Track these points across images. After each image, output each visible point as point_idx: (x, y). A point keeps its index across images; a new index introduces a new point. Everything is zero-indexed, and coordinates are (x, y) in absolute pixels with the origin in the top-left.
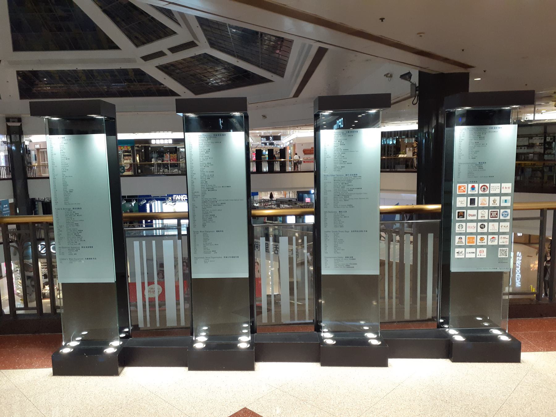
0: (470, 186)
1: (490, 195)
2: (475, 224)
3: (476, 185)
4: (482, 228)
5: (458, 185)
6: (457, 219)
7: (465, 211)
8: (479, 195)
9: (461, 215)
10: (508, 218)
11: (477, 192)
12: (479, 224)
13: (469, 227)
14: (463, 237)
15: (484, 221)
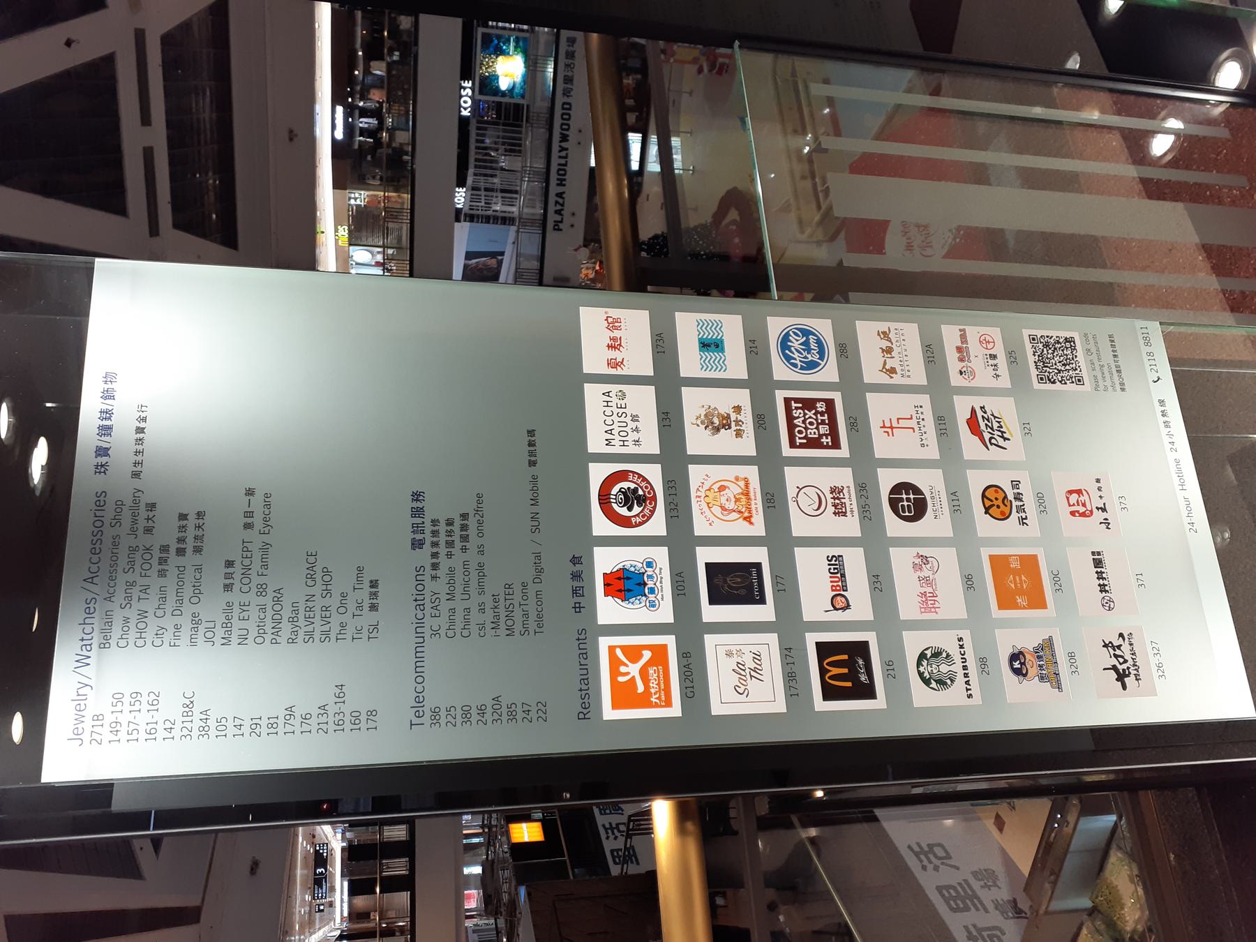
0: (609, 610)
1: (674, 456)
2: (901, 560)
3: (605, 561)
4: (919, 510)
5: (609, 713)
6: (880, 703)
7: (812, 639)
8: (681, 539)
9: (847, 669)
10: (823, 327)
11: (661, 555)
12: (894, 526)
13: (928, 600)
15: (865, 488)
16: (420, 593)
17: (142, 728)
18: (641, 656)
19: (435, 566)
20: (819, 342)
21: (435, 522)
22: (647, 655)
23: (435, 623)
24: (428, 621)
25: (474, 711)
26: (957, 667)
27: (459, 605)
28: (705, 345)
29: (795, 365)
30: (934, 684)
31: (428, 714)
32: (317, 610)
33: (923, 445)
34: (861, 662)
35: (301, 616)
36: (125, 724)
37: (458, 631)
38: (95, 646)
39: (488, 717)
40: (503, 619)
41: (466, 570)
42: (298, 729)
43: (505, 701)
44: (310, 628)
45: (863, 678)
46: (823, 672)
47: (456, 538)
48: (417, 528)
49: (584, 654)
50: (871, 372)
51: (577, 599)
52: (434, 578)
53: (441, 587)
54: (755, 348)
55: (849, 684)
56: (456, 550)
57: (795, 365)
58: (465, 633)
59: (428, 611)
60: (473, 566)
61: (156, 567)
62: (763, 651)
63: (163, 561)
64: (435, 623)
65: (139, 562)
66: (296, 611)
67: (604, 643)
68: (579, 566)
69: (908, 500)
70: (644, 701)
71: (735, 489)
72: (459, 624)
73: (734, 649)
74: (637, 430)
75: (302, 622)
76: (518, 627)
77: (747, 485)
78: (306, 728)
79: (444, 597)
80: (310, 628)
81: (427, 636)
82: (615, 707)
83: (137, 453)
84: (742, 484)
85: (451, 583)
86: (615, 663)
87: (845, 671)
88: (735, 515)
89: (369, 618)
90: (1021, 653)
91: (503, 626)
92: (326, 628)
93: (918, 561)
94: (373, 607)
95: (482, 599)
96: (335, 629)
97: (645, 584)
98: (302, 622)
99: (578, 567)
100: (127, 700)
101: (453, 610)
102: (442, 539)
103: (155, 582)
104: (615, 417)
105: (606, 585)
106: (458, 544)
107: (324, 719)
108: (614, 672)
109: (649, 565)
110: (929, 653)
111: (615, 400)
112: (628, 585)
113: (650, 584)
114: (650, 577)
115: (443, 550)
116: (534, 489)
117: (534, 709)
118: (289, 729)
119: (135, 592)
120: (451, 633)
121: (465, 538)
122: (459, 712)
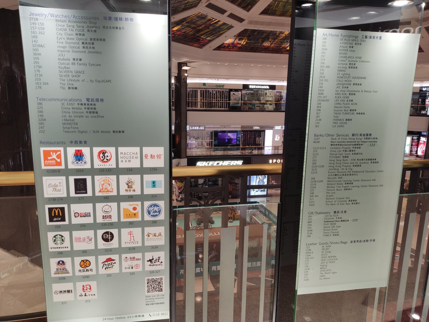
0: (71, 151)
1: (118, 171)
2: (91, 233)
3: (86, 151)
4: (106, 240)
5: (42, 149)
6: (48, 223)
7: (66, 206)
8: (93, 172)
9: (57, 215)
12: (100, 232)
13: (79, 240)
14: (68, 260)
15: (111, 225)
16: (74, 100)
17: (35, 30)
18: (58, 158)
19: (82, 104)
20: (157, 215)
21: (95, 105)
22: (59, 160)
23: (66, 104)
24: (66, 102)
25: (41, 114)
26: (59, 246)
27: (71, 110)
28: (154, 182)
29: (149, 208)
30: (54, 238)
31: (41, 102)
32: (68, 74)
33: (126, 243)
34: (60, 219)
35: (66, 70)
36: (35, 26)
37: (63, 110)
38: (56, 18)
39: (40, 117)
40: (67, 122)
41: (81, 113)
42: (36, 69)
43: (44, 122)
44: (63, 72)
45: (55, 219)
46: (56, 208)
47: (90, 110)
48: (92, 100)
49: (58, 143)
50: (147, 230)
51: (74, 142)
52: (78, 104)
53: (76, 106)
54: (154, 197)
55: (53, 215)
56: (87, 110)
57: (149, 208)
58: (63, 112)
59: (69, 102)
60: (82, 114)
61: (78, 33)
62: (62, 192)
63: (80, 34)
64: (66, 104)
65: (80, 28)
66: (68, 68)
67: (62, 149)
68: (85, 143)
69: (108, 237)
70: (46, 159)
71: (109, 188)
72: (65, 110)
73: (62, 184)
74: (126, 161)
75: (65, 70)
76: (65, 126)
77: (110, 192)
78: (36, 71)
79: (73, 106)
80: (63, 72)
81: (62, 102)
82: (44, 151)
83: (110, 27)
84: (111, 190)
85: (77, 108)
86: (56, 152)
87: (57, 214)
88: (101, 188)
89: (66, 87)
90: (64, 264)
91: (65, 122)
92: (63, 76)
93: (90, 238)
94: (69, 88)
95: (73, 116)
96: (63, 78)
97: (79, 161)
98: (65, 70)
99: (83, 143)
100: (42, 26)
101: (69, 109)
102: (90, 107)
103: (74, 33)
104: (129, 155)
105: (78, 150)
106: (88, 111)
107: (39, 75)
108: (53, 151)
109: (85, 163)
110: (63, 238)
111: (135, 156)
112: (79, 157)
113: (79, 162)
114: (81, 162)
115: (87, 106)
116: (106, 132)
117: (43, 129)
118: (36, 67)
119: (71, 28)
120: (63, 108)
121: (90, 112)
122: (41, 110)
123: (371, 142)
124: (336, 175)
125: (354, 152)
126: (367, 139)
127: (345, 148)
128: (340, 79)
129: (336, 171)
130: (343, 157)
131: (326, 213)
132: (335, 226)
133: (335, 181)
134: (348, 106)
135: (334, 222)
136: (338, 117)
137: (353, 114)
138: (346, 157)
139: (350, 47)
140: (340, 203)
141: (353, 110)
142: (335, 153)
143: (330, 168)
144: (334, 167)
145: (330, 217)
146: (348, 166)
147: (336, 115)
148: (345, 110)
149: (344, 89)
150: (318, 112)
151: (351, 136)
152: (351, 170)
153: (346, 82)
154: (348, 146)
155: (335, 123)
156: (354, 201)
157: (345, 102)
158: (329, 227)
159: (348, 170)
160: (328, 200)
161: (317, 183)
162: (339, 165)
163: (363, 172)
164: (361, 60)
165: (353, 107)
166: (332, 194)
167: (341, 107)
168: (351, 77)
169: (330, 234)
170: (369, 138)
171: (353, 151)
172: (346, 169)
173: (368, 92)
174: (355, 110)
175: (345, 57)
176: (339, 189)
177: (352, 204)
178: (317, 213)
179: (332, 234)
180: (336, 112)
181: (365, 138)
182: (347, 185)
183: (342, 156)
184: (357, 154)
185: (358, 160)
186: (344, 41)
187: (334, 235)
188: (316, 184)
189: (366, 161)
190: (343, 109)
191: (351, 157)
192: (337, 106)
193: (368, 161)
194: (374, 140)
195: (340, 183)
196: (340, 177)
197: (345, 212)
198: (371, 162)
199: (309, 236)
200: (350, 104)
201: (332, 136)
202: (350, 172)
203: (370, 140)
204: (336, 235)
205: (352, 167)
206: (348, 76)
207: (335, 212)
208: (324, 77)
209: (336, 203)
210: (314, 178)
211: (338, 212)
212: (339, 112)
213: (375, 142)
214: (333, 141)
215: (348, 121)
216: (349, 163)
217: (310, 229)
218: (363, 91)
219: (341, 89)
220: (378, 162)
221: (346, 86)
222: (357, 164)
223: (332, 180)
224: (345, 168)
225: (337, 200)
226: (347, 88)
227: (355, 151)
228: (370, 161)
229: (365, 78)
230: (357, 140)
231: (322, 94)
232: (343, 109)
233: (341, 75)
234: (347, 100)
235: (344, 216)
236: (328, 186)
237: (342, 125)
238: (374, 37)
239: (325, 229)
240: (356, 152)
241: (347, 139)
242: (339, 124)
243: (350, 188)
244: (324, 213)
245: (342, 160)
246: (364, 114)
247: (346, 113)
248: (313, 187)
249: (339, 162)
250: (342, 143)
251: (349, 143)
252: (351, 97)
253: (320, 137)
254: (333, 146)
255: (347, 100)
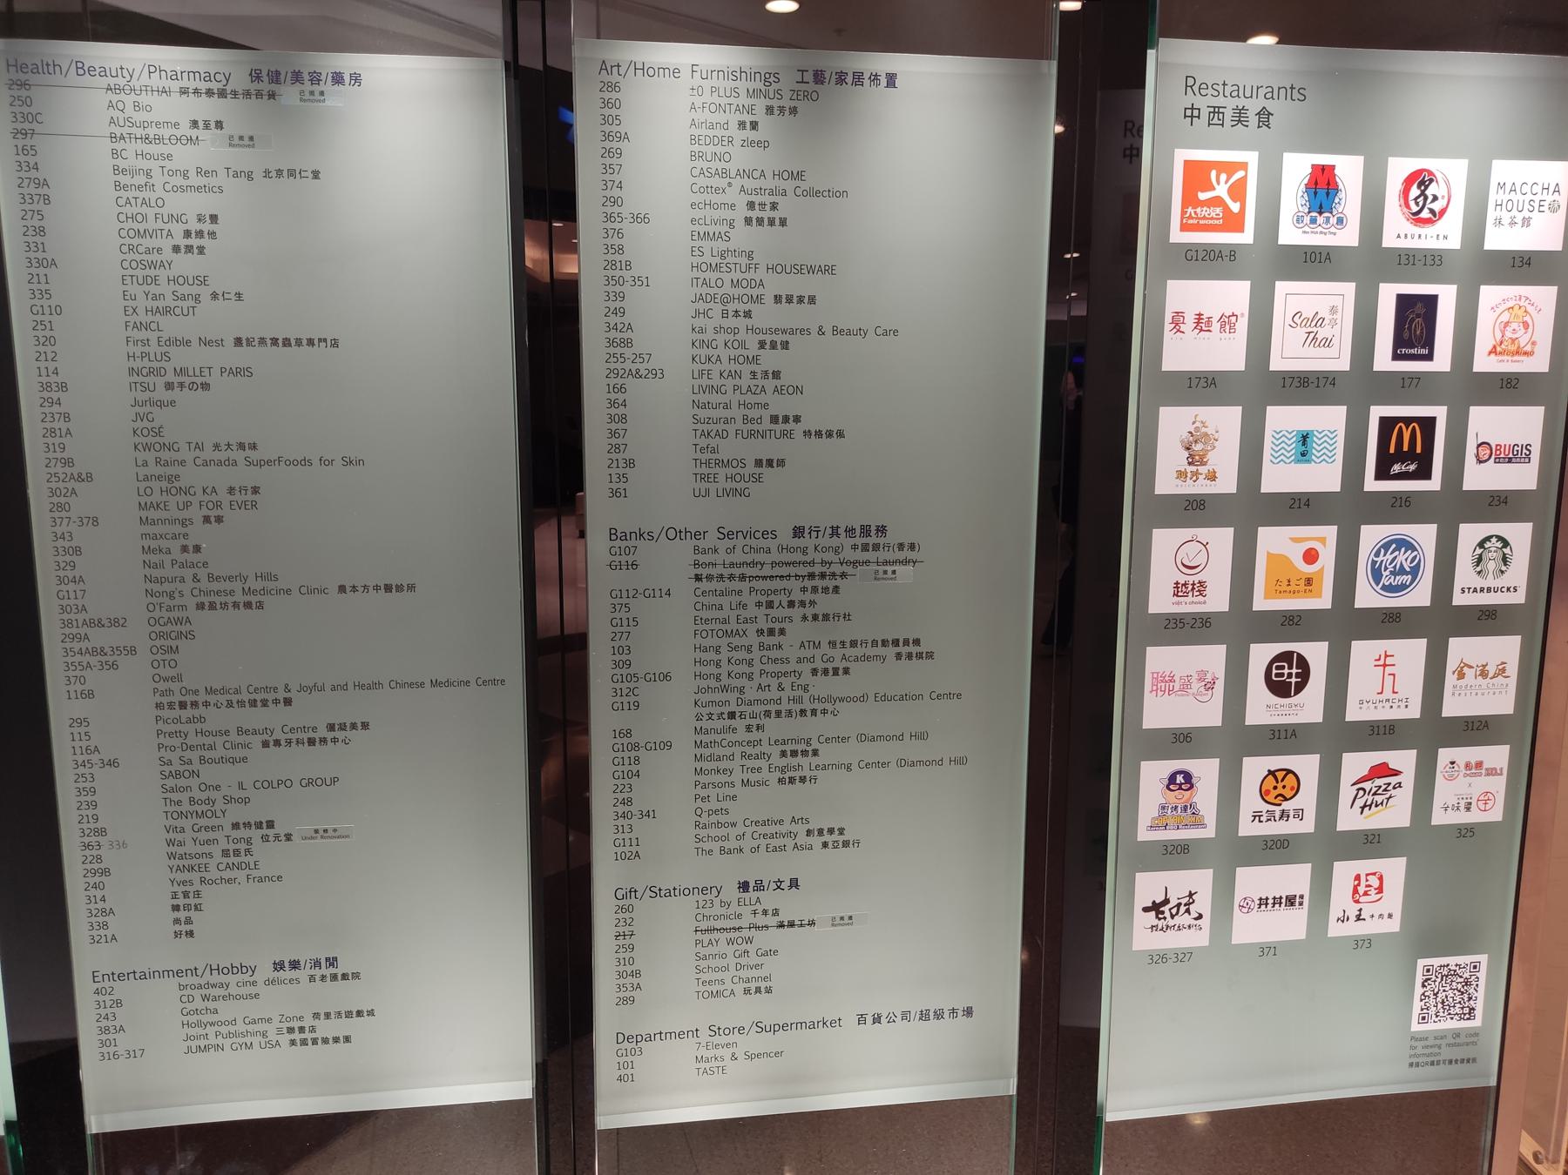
123: (886, 563)
124: (732, 715)
125: (809, 611)
126: (865, 548)
127: (766, 592)
128: (708, 275)
129: (732, 697)
130: (760, 632)
131: (703, 890)
132: (751, 948)
133: (732, 744)
134: (761, 399)
135: (745, 933)
136: (714, 451)
137: (787, 434)
138: (771, 632)
139: (742, 125)
140: (763, 842)
141: (786, 419)
142: (720, 615)
143: (704, 684)
144: (718, 678)
145: (723, 911)
146: (785, 674)
147: (703, 442)
148: (745, 419)
149: (731, 322)
150: (614, 426)
151: (785, 537)
152: (806, 689)
153: (741, 291)
154: (778, 584)
155: (704, 478)
156: (831, 831)
157: (745, 381)
158: (724, 956)
159: (788, 692)
160: (703, 833)
161: (642, 753)
162: (744, 668)
163: (863, 698)
164: (805, 186)
165: (781, 405)
166: (724, 805)
167: (726, 407)
168: (762, 268)
169: (729, 985)
170: (876, 547)
171: (802, 604)
172: (781, 688)
173: (849, 333)
174: (797, 419)
175: (724, 173)
176: (753, 777)
177: (825, 845)
178: (656, 893)
179: (739, 988)
180: (706, 427)
181: (855, 547)
182: (790, 760)
183: (751, 629)
184: (826, 617)
185: (832, 644)
186: (707, 98)
187: (747, 991)
188: (637, 759)
189: (871, 651)
190: (736, 413)
191: (798, 631)
192: (704, 398)
193: (880, 650)
194: (901, 555)
195: (758, 750)
196: (754, 722)
197: (794, 883)
198: (899, 656)
199: (625, 1001)
200: (770, 390)
201: (696, 535)
202: (799, 700)
203: (883, 555)
204: (758, 990)
205: (807, 678)
206: (744, 261)
207: (744, 886)
208: (628, 264)
209: (747, 844)
210: (629, 732)
211: (759, 886)
212: (720, 427)
213: (906, 562)
214: (702, 558)
215: (764, 470)
216: (793, 660)
217: (629, 969)
218: (828, 329)
219: (717, 320)
220: (930, 655)
221: (742, 308)
222: (830, 666)
223: (718, 738)
224: (774, 683)
225: (749, 830)
226: (748, 314)
227: (813, 603)
228: (891, 651)
229: (829, 270)
230: (818, 557)
231: (628, 343)
232: (736, 413)
233: (707, 258)
234: (754, 373)
235: (791, 905)
236: (698, 765)
237: (740, 486)
238: (858, 78)
239: (703, 964)
240: (819, 610)
241: (769, 551)
242: (723, 483)
243: (806, 773)
244: (691, 891)
245: (755, 648)
246: (841, 434)
247: (751, 434)
248: (629, 774)
249: (742, 655)
250: (749, 571)
251: (784, 571)
252: (770, 360)
253: (640, 543)
254: (705, 585)
255: (754, 373)
